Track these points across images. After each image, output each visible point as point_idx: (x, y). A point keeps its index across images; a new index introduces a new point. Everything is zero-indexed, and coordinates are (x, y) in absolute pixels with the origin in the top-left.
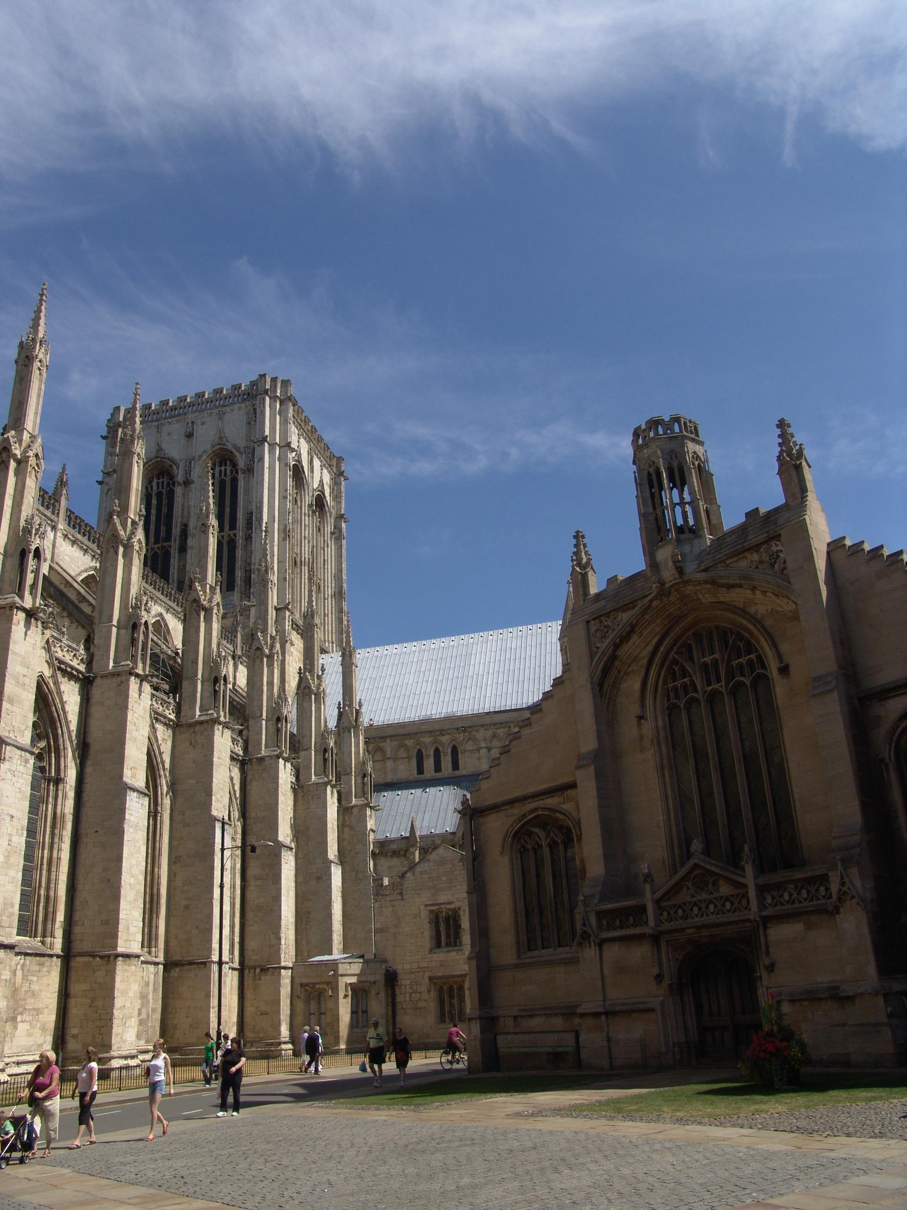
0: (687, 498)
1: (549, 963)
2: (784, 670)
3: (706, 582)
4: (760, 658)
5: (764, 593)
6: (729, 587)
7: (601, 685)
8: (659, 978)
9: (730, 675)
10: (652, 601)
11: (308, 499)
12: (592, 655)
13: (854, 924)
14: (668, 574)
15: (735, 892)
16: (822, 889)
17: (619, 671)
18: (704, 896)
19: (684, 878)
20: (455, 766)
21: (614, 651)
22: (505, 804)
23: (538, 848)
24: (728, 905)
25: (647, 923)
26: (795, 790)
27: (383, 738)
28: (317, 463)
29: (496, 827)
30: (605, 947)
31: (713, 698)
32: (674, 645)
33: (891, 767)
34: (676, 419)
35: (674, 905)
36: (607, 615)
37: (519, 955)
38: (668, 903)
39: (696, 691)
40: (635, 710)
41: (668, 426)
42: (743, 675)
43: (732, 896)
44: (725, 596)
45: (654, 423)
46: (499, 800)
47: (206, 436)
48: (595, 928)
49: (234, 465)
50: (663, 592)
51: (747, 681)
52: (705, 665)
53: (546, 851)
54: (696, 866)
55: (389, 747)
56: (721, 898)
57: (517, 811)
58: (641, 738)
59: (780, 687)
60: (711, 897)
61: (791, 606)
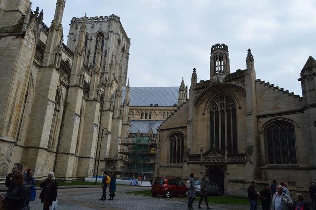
0: (222, 64)
2: (240, 108)
4: (234, 104)
6: (229, 87)
8: (201, 173)
11: (121, 48)
20: (150, 118)
22: (168, 129)
23: (175, 140)
27: (133, 109)
28: (124, 39)
29: (166, 134)
34: (223, 45)
40: (203, 112)
41: (221, 46)
45: (218, 45)
46: (167, 128)
47: (97, 28)
49: (103, 37)
50: (214, 86)
53: (177, 141)
54: (213, 149)
55: (135, 112)
58: (203, 119)
59: (238, 112)
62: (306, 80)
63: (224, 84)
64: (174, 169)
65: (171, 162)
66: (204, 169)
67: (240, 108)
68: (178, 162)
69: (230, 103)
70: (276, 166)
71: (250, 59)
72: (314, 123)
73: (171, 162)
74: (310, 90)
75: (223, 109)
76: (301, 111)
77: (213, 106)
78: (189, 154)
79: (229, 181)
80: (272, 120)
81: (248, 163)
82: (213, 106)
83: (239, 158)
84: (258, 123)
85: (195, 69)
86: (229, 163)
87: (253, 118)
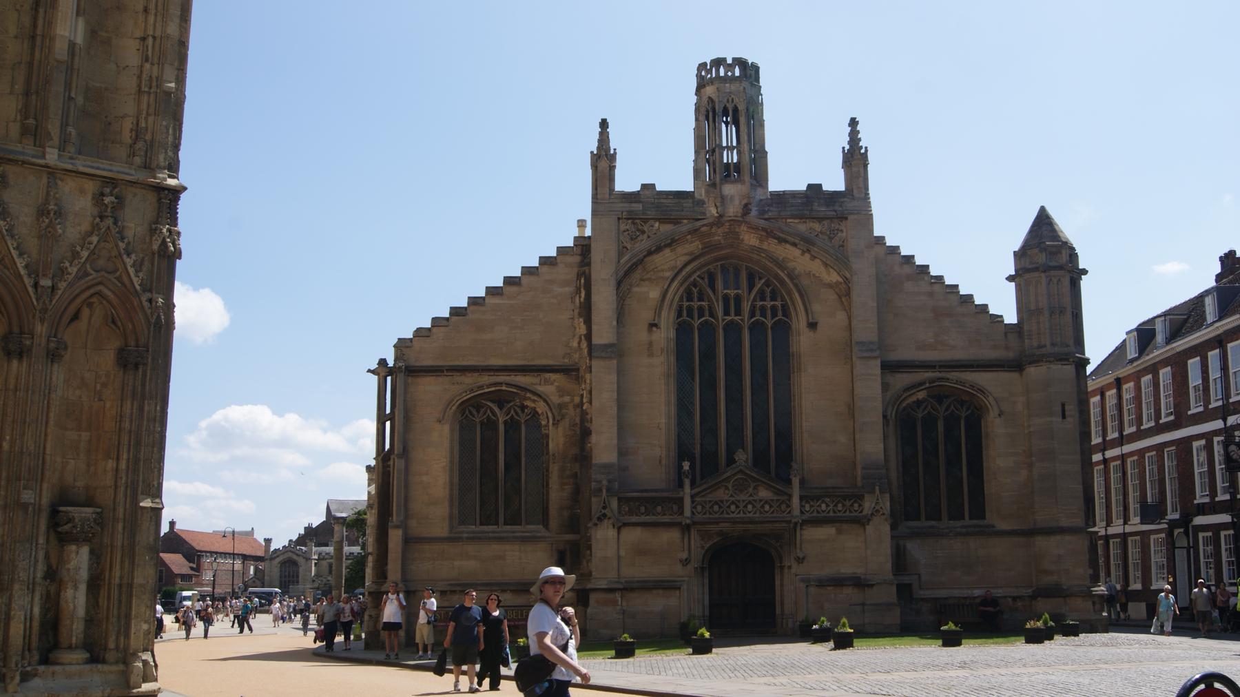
1: (500, 540)
2: (813, 326)
3: (764, 230)
4: (785, 308)
6: (781, 241)
7: (619, 283)
8: (686, 562)
9: (752, 314)
12: (620, 254)
13: (880, 532)
14: (733, 210)
15: (775, 498)
16: (856, 505)
25: (682, 513)
32: (699, 269)
37: (451, 528)
40: (647, 315)
42: (763, 314)
44: (772, 246)
48: (616, 512)
51: (769, 323)
52: (726, 299)
53: (501, 428)
54: (741, 471)
57: (469, 380)
58: (650, 344)
61: (834, 277)
63: (756, 228)
64: (495, 548)
66: (697, 546)
67: (813, 326)
68: (514, 519)
69: (763, 299)
71: (855, 160)
72: (1059, 409)
74: (1052, 313)
76: (1017, 366)
77: (690, 299)
79: (807, 582)
80: (921, 384)
82: (690, 299)
84: (885, 387)
85: (604, 124)
86: (805, 522)
87: (875, 368)
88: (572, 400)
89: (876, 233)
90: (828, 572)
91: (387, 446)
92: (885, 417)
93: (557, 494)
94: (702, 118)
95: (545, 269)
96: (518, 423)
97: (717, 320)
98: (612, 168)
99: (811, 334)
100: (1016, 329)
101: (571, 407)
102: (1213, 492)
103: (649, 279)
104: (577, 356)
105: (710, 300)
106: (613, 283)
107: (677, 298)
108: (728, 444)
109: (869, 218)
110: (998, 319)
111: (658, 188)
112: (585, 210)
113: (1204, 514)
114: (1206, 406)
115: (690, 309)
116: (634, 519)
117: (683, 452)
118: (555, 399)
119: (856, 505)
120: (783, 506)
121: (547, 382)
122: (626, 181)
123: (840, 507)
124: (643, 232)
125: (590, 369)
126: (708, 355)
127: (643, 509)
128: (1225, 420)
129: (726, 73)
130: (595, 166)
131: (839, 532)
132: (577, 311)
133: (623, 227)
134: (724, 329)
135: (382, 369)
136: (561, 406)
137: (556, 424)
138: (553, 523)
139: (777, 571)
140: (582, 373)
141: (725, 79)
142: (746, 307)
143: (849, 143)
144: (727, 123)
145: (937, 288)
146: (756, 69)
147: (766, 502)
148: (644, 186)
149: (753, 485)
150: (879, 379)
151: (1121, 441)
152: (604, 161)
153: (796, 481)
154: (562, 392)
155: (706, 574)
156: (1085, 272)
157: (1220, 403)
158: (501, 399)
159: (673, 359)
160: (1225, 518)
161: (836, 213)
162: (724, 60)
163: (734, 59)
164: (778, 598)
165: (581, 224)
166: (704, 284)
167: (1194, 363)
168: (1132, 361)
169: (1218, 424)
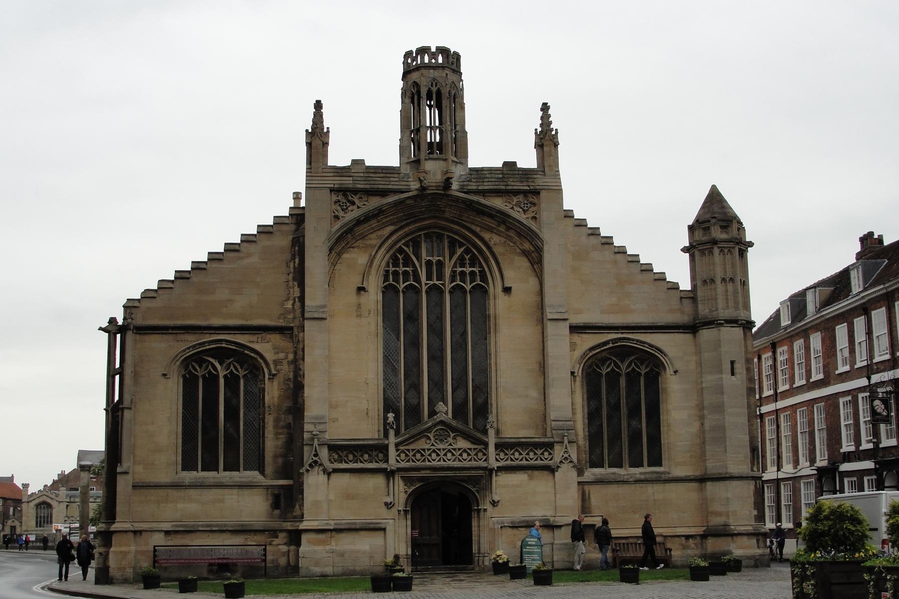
2: (507, 290)
3: (464, 201)
5: (508, 229)
7: (331, 250)
8: (389, 506)
9: (453, 279)
10: (409, 198)
16: (546, 454)
17: (348, 243)
18: (441, 446)
19: (429, 430)
21: (355, 225)
24: (465, 455)
25: (387, 461)
26: (502, 381)
30: (334, 477)
31: (432, 289)
32: (403, 238)
33: (578, 378)
35: (413, 450)
36: (355, 192)
38: (407, 447)
39: (417, 278)
40: (356, 282)
43: (470, 449)
45: (443, 51)
51: (468, 287)
52: (429, 264)
53: (222, 381)
54: (442, 422)
56: (459, 449)
57: (192, 339)
58: (359, 306)
60: (450, 447)
61: (527, 246)
62: (716, 251)
65: (188, 464)
66: (400, 491)
67: (507, 290)
68: (231, 466)
69: (463, 265)
70: (613, 474)
71: (546, 141)
73: (184, 468)
74: (724, 280)
75: (437, 283)
76: (692, 328)
78: (327, 436)
81: (565, 467)
82: (396, 264)
83: (533, 453)
84: (573, 347)
85: (318, 105)
86: (500, 469)
87: (564, 328)
88: (286, 358)
89: (566, 207)
90: (519, 515)
91: (117, 398)
92: (572, 373)
93: (272, 443)
94: (408, 100)
95: (263, 236)
96: (238, 377)
97: (420, 283)
98: (325, 144)
99: (506, 297)
100: (692, 296)
101: (285, 362)
102: (858, 442)
103: (358, 247)
104: (291, 316)
105: (414, 266)
106: (326, 250)
107: (384, 264)
108: (429, 398)
109: (559, 191)
110: (675, 287)
111: (368, 163)
112: (295, 178)
113: (849, 461)
114: (852, 366)
115: (396, 273)
116: (343, 466)
117: (389, 405)
118: (270, 356)
119: (546, 454)
120: (480, 455)
121: (263, 340)
122: (338, 156)
123: (531, 454)
124: (353, 203)
125: (302, 328)
126: (412, 317)
127: (351, 457)
128: (869, 378)
129: (430, 60)
130: (309, 145)
131: (531, 478)
132: (291, 276)
133: (334, 198)
134: (427, 292)
135: (112, 329)
136: (276, 362)
137: (272, 376)
138: (269, 469)
139: (474, 515)
140: (295, 330)
141: (428, 67)
142: (448, 272)
143: (541, 125)
144: (430, 107)
145: (619, 256)
146: (457, 57)
147: (465, 451)
148: (354, 162)
149: (452, 435)
150: (568, 339)
151: (775, 397)
152: (317, 139)
153: (491, 433)
154: (277, 350)
155: (409, 517)
156: (751, 244)
157: (865, 363)
158: (221, 354)
159: (380, 319)
160: (869, 465)
161: (529, 187)
162: (429, 48)
163: (438, 48)
164: (475, 538)
165: (297, 196)
166: (410, 251)
167: (841, 331)
168: (786, 328)
169: (864, 382)
